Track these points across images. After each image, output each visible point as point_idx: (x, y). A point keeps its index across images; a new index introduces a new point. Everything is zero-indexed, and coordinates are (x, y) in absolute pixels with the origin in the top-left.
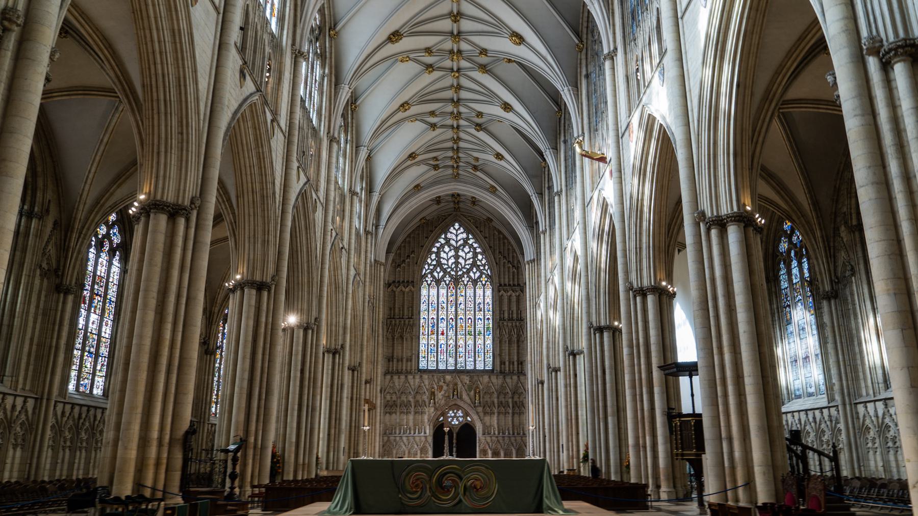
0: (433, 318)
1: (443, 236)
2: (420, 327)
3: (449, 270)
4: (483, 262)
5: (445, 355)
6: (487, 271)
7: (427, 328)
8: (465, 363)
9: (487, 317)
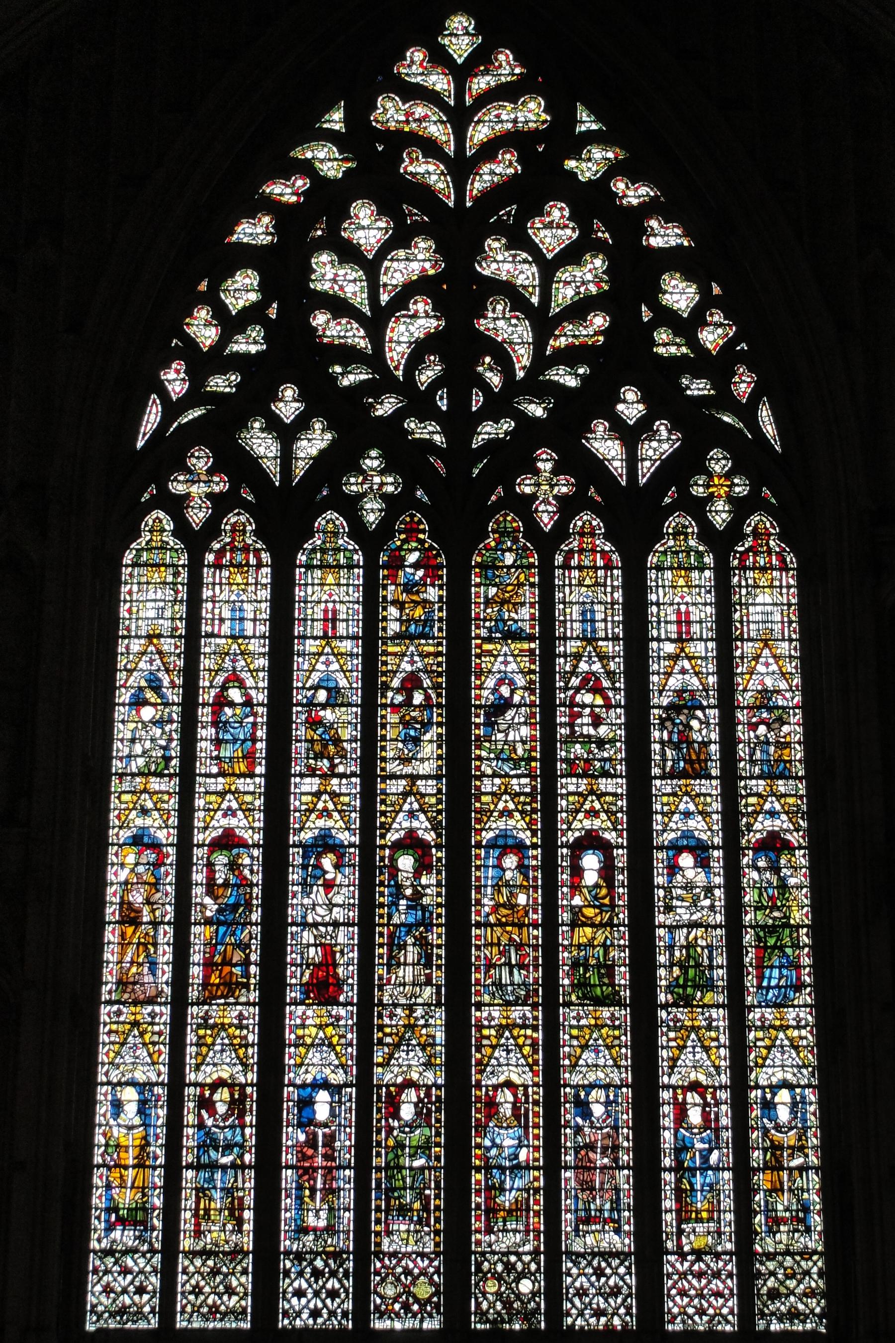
1: (336, 120)
2: (101, 924)
3: (386, 407)
5: (348, 1198)
6: (748, 413)
7: (166, 935)
8: (554, 1275)
9: (763, 825)
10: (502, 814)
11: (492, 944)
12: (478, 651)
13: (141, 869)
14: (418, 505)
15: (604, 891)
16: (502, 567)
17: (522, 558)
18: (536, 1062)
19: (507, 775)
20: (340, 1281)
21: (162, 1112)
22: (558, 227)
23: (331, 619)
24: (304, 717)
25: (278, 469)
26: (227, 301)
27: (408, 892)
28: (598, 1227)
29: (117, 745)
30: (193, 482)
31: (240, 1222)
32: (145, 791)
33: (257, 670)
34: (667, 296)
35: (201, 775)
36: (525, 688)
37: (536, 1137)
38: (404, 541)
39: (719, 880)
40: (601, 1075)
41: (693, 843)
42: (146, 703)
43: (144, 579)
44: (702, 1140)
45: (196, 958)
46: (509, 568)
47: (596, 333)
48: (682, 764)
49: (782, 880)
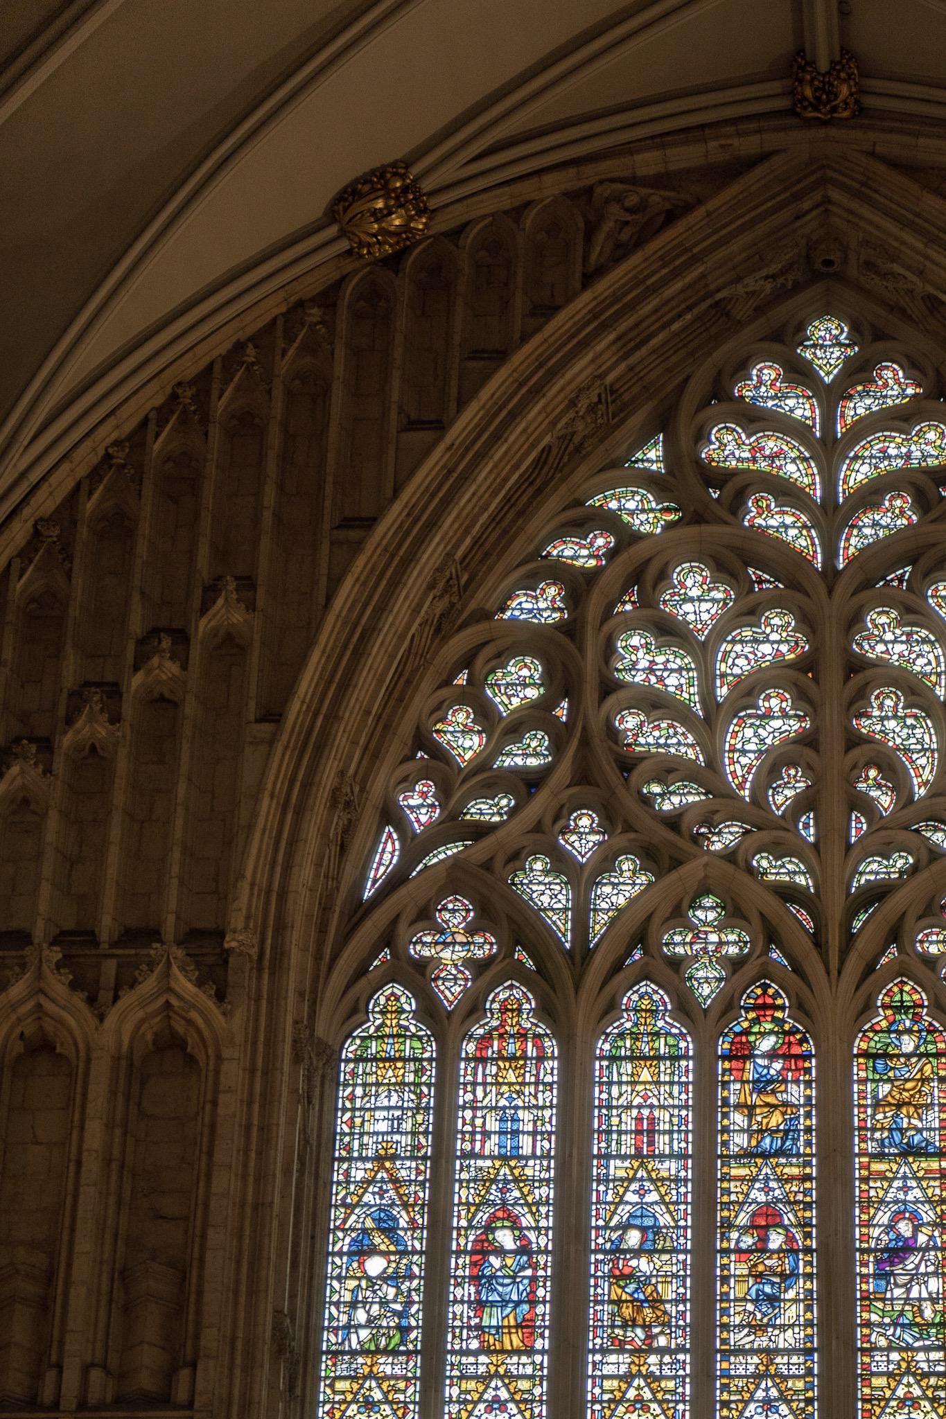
3: (726, 838)
12: (865, 1173)
16: (898, 1056)
17: (926, 1042)
19: (909, 1348)
25: (569, 925)
26: (497, 700)
32: (371, 1376)
33: (537, 1204)
35: (453, 1352)
42: (373, 1251)
43: (372, 1079)
46: (908, 1056)
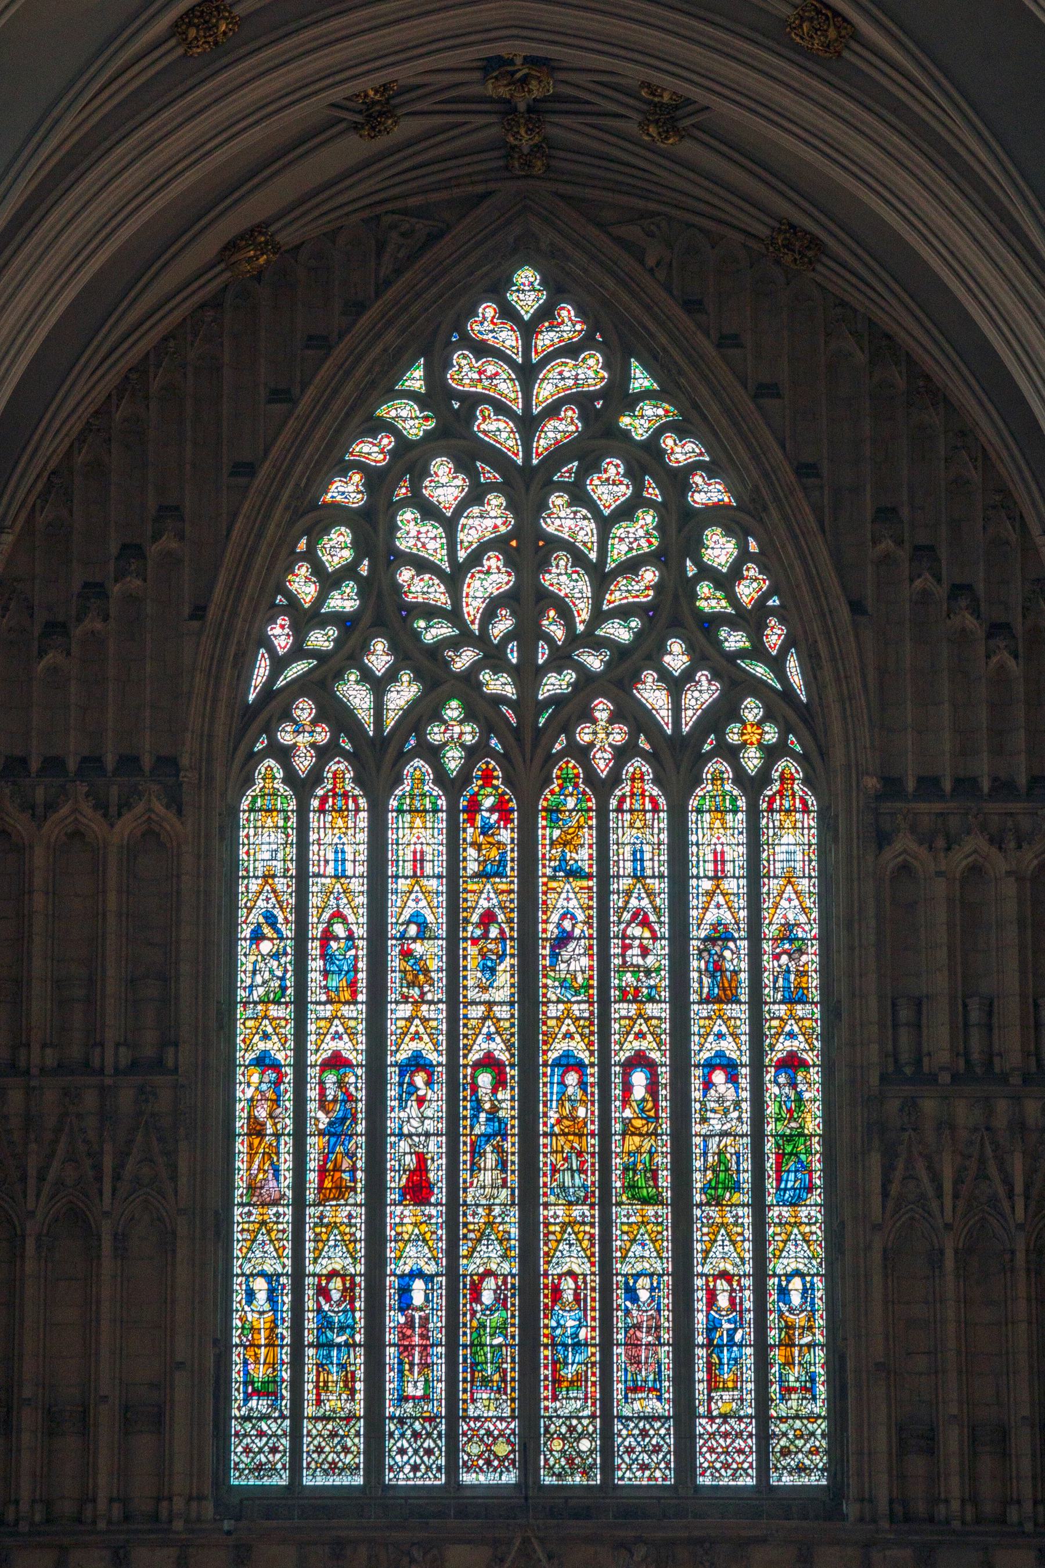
0: (336, 1062)
1: (415, 379)
2: (230, 1136)
3: (464, 659)
4: (747, 591)
5: (440, 1370)
6: (777, 665)
7: (286, 1145)
8: (607, 1435)
9: (784, 1046)
10: (564, 1037)
11: (557, 1152)
13: (264, 1087)
14: (492, 753)
15: (650, 1105)
18: (593, 1254)
19: (569, 1001)
20: (434, 1441)
21: (287, 1299)
22: (614, 484)
23: (419, 860)
24: (398, 949)
26: (324, 559)
27: (487, 1106)
28: (644, 1395)
29: (241, 976)
30: (299, 733)
31: (353, 1392)
32: (266, 1017)
33: (357, 907)
34: (709, 551)
36: (585, 923)
37: (593, 1319)
38: (482, 787)
39: (745, 1095)
40: (647, 1266)
41: (725, 1062)
42: (264, 937)
44: (729, 1321)
45: (312, 1165)
46: (571, 811)
47: (647, 588)
48: (716, 991)
49: (799, 1094)
